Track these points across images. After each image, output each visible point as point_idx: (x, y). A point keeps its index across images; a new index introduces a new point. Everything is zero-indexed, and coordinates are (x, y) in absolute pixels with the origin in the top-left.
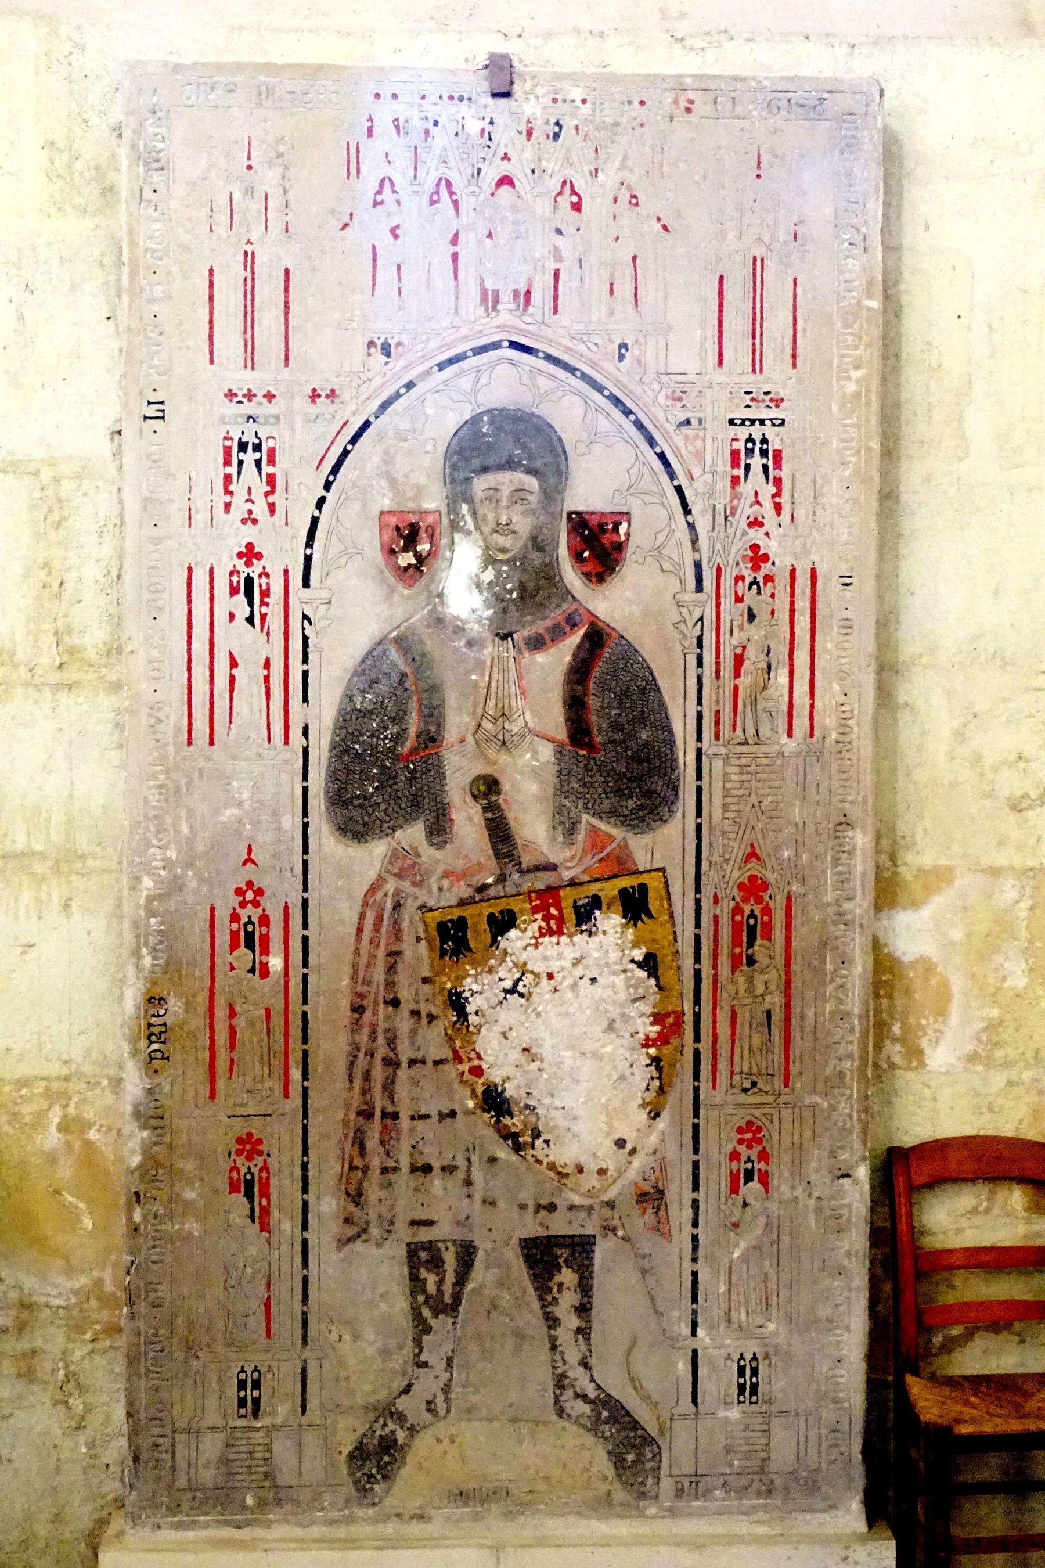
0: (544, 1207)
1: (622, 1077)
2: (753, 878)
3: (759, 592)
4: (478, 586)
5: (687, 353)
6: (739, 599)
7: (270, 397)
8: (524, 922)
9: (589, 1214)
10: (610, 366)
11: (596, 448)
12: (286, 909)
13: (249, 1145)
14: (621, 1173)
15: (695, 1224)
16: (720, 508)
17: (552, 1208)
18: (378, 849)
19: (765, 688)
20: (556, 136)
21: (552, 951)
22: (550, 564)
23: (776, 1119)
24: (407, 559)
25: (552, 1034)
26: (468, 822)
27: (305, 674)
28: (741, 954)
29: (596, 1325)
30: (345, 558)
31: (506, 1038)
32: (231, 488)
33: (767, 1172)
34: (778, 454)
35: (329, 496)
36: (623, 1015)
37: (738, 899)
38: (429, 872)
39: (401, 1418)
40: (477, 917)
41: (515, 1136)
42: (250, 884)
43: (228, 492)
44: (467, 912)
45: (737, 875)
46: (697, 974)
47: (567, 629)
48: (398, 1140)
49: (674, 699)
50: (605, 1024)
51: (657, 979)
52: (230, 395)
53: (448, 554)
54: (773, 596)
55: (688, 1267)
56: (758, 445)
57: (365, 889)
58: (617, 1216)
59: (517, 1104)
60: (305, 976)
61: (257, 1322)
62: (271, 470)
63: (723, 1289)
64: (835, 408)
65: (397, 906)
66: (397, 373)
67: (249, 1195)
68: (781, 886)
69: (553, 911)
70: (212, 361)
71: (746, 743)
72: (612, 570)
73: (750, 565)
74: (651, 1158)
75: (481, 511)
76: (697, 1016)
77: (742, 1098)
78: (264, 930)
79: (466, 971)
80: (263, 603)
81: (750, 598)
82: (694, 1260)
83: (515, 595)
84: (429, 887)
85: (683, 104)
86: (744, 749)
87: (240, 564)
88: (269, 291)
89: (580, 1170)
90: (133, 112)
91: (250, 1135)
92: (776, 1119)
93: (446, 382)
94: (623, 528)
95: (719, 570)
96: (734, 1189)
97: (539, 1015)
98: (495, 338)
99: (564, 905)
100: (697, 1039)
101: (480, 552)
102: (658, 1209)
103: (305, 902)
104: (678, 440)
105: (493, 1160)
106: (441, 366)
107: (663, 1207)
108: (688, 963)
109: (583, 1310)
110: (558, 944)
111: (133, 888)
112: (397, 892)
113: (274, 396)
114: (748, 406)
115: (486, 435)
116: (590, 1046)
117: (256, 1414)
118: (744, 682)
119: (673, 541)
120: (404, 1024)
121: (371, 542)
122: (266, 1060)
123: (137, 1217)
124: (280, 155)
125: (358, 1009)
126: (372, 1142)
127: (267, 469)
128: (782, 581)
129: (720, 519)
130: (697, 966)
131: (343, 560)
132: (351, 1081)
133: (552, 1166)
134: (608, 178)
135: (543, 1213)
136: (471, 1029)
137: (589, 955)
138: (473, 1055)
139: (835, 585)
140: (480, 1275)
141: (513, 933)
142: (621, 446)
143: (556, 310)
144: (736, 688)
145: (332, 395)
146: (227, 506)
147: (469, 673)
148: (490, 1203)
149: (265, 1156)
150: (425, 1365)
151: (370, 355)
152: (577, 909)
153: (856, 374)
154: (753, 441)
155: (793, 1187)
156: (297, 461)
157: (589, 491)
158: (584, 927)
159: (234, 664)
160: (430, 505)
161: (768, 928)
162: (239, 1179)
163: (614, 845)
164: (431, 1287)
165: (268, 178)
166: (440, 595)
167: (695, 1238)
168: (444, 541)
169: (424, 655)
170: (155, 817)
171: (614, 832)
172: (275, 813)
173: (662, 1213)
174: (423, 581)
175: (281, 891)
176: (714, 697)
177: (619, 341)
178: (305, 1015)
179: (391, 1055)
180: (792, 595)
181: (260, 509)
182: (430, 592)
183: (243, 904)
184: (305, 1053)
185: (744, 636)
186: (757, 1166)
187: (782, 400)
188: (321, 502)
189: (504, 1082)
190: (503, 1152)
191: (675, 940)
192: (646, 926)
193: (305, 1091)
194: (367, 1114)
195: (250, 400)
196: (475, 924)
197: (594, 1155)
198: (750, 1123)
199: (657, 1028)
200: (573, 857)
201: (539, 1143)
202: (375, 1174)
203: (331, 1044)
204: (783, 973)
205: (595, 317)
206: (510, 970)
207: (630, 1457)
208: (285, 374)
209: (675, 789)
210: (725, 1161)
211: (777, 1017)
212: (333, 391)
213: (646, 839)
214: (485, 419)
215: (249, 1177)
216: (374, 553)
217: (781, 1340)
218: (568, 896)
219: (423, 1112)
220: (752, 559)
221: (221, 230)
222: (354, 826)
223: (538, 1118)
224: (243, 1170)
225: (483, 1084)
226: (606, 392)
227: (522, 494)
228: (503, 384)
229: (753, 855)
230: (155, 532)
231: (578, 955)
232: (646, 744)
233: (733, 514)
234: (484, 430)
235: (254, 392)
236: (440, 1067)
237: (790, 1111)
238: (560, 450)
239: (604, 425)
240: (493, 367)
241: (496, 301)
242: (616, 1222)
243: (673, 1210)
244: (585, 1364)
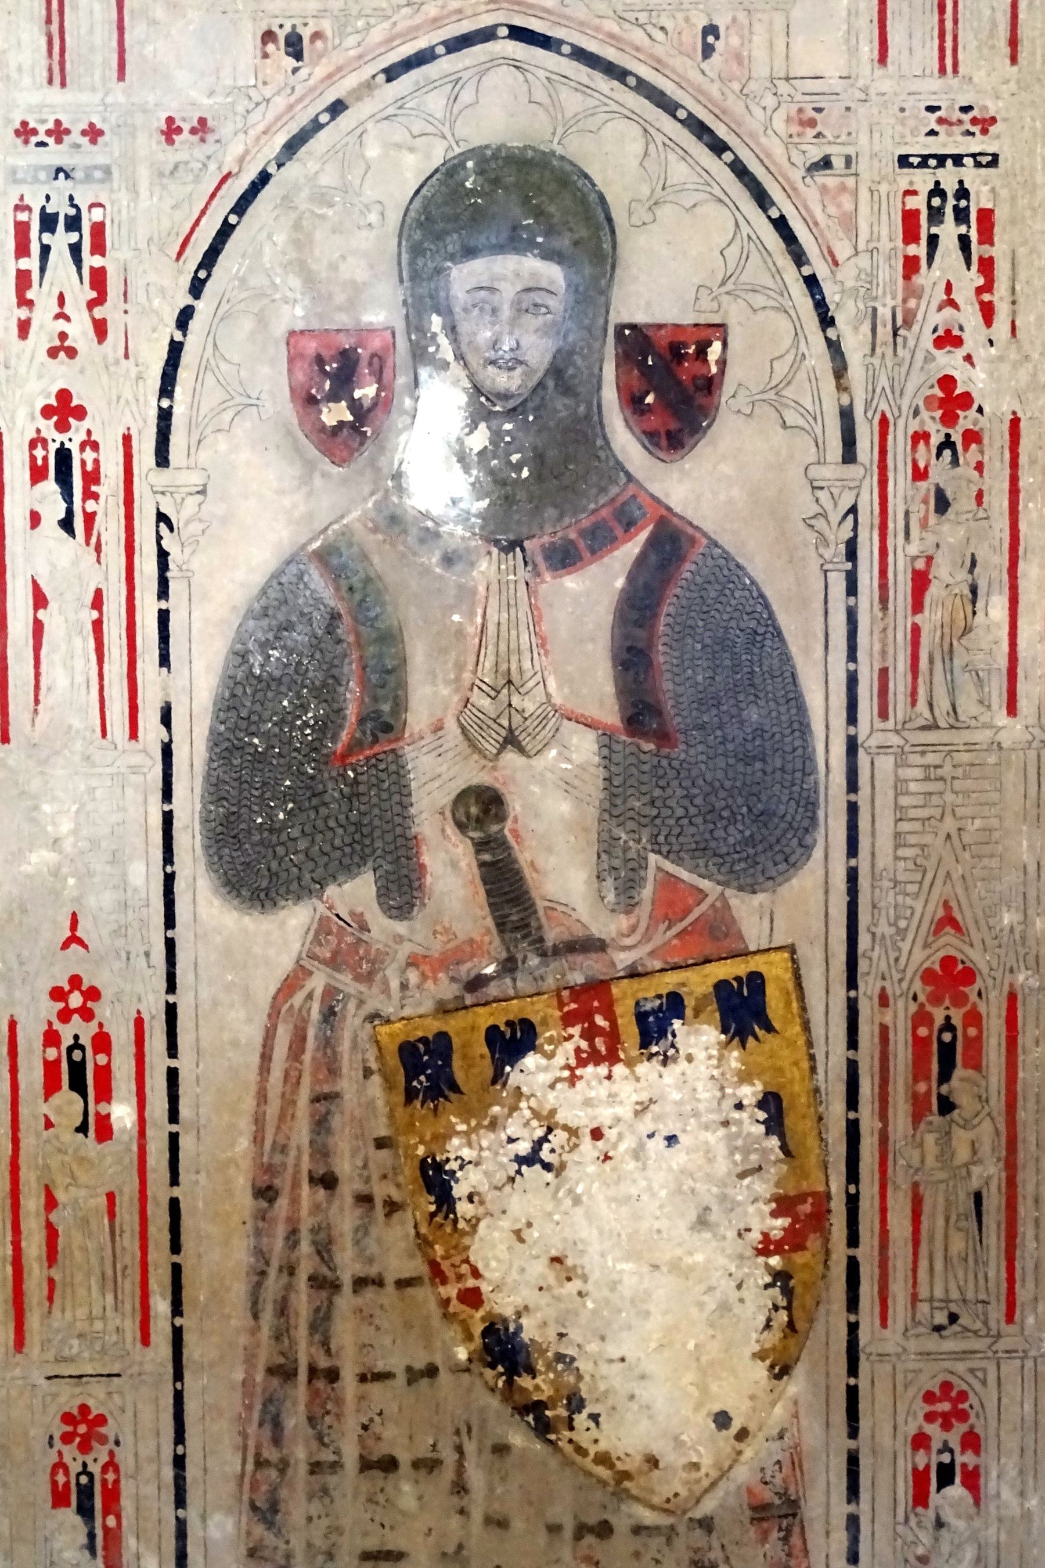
0: (591, 1530)
1: (724, 1307)
2: (948, 962)
3: (955, 462)
4: (462, 458)
6: (919, 474)
7: (93, 133)
8: (550, 1041)
9: (669, 1541)
10: (689, 67)
11: (665, 212)
12: (139, 1023)
13: (83, 1426)
16: (884, 313)
17: (604, 1530)
18: (296, 920)
19: (967, 630)
21: (602, 1091)
22: (588, 417)
23: (992, 1377)
24: (335, 413)
25: (601, 1232)
26: (449, 867)
27: (164, 617)
28: (928, 1093)
30: (230, 413)
31: (522, 1240)
32: (30, 295)
33: (977, 1468)
34: (986, 217)
35: (200, 305)
37: (922, 998)
40: (469, 1031)
41: (538, 1407)
42: (75, 981)
43: (24, 302)
44: (453, 1025)
45: (921, 957)
46: (853, 1130)
47: (619, 531)
48: (338, 1416)
49: (807, 650)
50: (692, 1215)
51: (782, 1137)
52: (25, 132)
53: (408, 402)
54: (979, 467)
56: (951, 202)
57: (272, 990)
58: (716, 1544)
59: (543, 1352)
60: (174, 1138)
62: (97, 261)
65: (329, 1015)
66: (312, 90)
67: (85, 1511)
68: (998, 975)
69: (600, 1021)
71: (934, 726)
73: (938, 414)
74: (776, 1445)
75: (464, 328)
76: (853, 1202)
77: (932, 1343)
79: (452, 1126)
80: (89, 495)
81: (940, 472)
83: (525, 473)
84: (386, 982)
86: (931, 737)
87: (48, 428)
89: (653, 1462)
91: (84, 1409)
92: (992, 1377)
93: (400, 102)
94: (715, 350)
95: (884, 422)
96: (921, 1498)
97: (577, 1201)
98: (486, 21)
99: (619, 1010)
100: (853, 1240)
101: (463, 399)
102: (789, 1531)
103: (171, 1011)
104: (811, 194)
105: (501, 1449)
106: (391, 73)
107: (796, 1530)
108: (836, 1109)
110: (609, 1077)
112: (330, 992)
113: (101, 133)
114: (932, 133)
115: (472, 192)
116: (665, 1254)
118: (930, 619)
119: (802, 375)
120: (345, 1219)
121: (272, 383)
122: (111, 1283)
125: (266, 1193)
126: (294, 1420)
127: (90, 260)
128: (997, 438)
129: (884, 332)
130: (852, 1115)
131: (227, 416)
132: (256, 1316)
133: (604, 1459)
135: (589, 1539)
136: (462, 1225)
137: (663, 1097)
138: (465, 1269)
141: (531, 1060)
142: (711, 209)
144: (916, 630)
145: (202, 128)
146: (24, 328)
148: (498, 1523)
149: (111, 1445)
151: (266, 56)
152: (641, 1017)
154: (942, 194)
155: (1022, 1494)
156: (142, 245)
157: (654, 288)
158: (654, 1049)
159: (40, 600)
161: (975, 1045)
162: (67, 1484)
163: (704, 907)
166: (397, 476)
168: (402, 380)
169: (368, 581)
171: (705, 884)
172: (115, 859)
173: (795, 1540)
175: (130, 992)
176: (877, 647)
177: (702, 22)
178: (174, 1205)
179: (325, 1271)
180: (1014, 464)
181: (80, 330)
182: (377, 470)
183: (65, 1016)
184: (177, 1270)
185: (931, 539)
186: (959, 1459)
187: (993, 120)
189: (519, 1315)
190: (519, 1437)
191: (813, 1069)
192: (763, 1046)
193: (177, 1334)
194: (283, 1372)
195: (59, 141)
196: (465, 1045)
197: (676, 1439)
198: (946, 1386)
200: (633, 929)
201: (581, 1420)
203: (221, 1251)
204: (1002, 1128)
206: (527, 1124)
208: (118, 94)
210: (904, 1448)
211: (994, 1202)
212: (202, 121)
213: (761, 898)
214: (470, 164)
215: (84, 1479)
218: (626, 997)
219: (380, 1366)
220: (942, 403)
222: (255, 875)
223: (580, 1377)
224: (75, 1468)
225: (483, 1319)
226: (682, 114)
227: (538, 297)
228: (499, 105)
229: (948, 921)
231: (644, 1096)
232: (760, 731)
233: (908, 323)
234: (468, 185)
235: (66, 125)
236: (410, 1291)
237: (1018, 1363)
238: (602, 217)
239: (679, 171)
240: (482, 74)
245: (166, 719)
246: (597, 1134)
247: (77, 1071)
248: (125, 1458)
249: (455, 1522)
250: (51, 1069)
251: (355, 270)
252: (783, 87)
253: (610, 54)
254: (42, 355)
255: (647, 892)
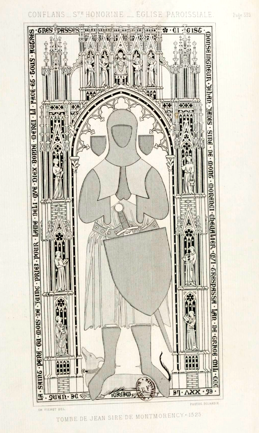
20: (133, 39)
67: (61, 316)
161: (193, 243)
198: (190, 294)
224: (60, 309)
250: (56, 248)
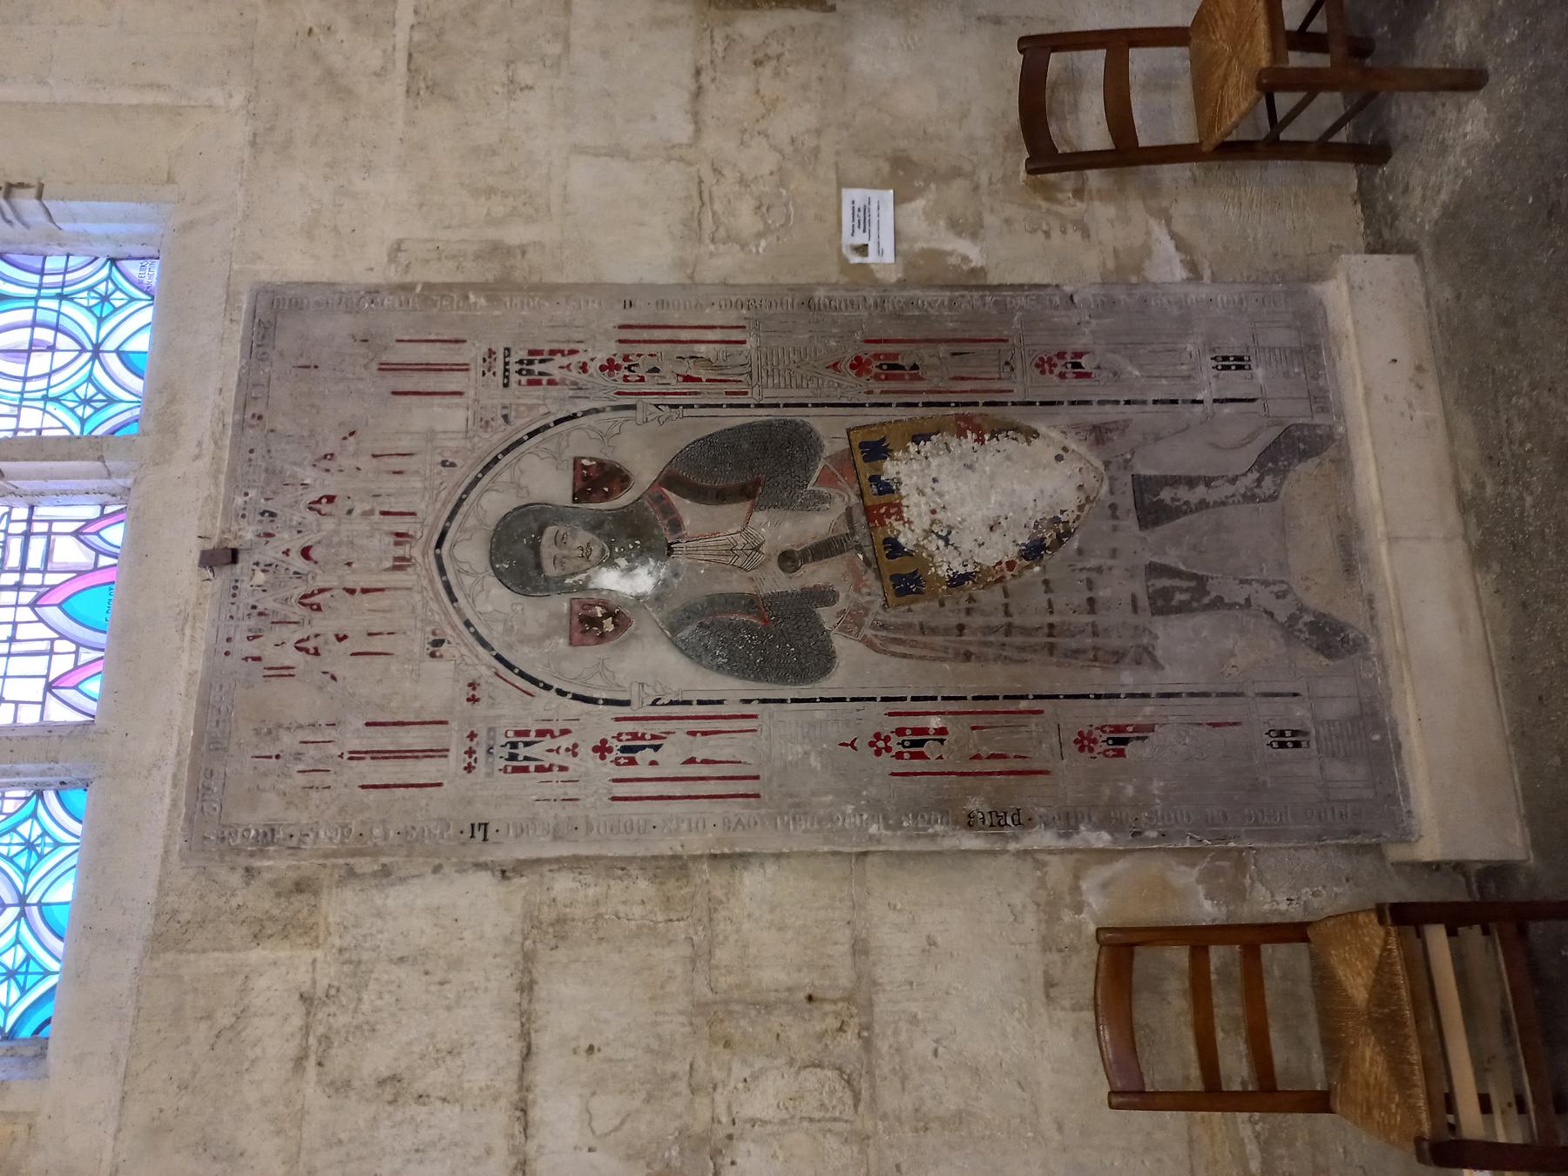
1: (1008, 458)
4: (630, 569)
5: (450, 418)
6: (642, 379)
7: (472, 736)
11: (523, 482)
12: (890, 714)
13: (1084, 742)
14: (1081, 458)
15: (1117, 402)
16: (571, 393)
18: (839, 643)
20: (272, 515)
21: (914, 510)
24: (608, 625)
26: (816, 575)
27: (700, 702)
29: (1203, 472)
34: (531, 353)
35: (556, 686)
36: (960, 458)
38: (856, 604)
39: (1293, 619)
42: (872, 744)
43: (550, 769)
44: (887, 574)
46: (927, 404)
50: (968, 472)
52: (469, 768)
55: (1150, 407)
60: (944, 698)
61: (1229, 734)
62: (533, 734)
63: (1164, 382)
64: (497, 313)
65: (884, 627)
67: (1125, 741)
70: (439, 785)
71: (750, 374)
72: (620, 470)
75: (572, 570)
77: (1018, 371)
78: (908, 732)
80: (643, 738)
81: (640, 371)
82: (1144, 402)
85: (255, 422)
87: (610, 757)
88: (382, 740)
90: (222, 855)
91: (1076, 742)
93: (466, 596)
94: (586, 462)
96: (1088, 375)
98: (432, 559)
100: (976, 404)
103: (884, 699)
105: (1080, 551)
106: (453, 600)
108: (919, 412)
109: (1191, 482)
111: (879, 841)
112: (873, 627)
117: (1306, 734)
118: (704, 374)
120: (977, 621)
121: (591, 654)
123: (1153, 834)
124: (270, 732)
125: (968, 656)
126: (1073, 644)
128: (627, 349)
129: (581, 393)
133: (1081, 508)
134: (309, 475)
139: (632, 312)
140: (1172, 558)
141: (902, 540)
142: (523, 464)
143: (413, 514)
145: (473, 685)
146: (563, 769)
147: (698, 574)
150: (1248, 600)
152: (880, 493)
153: (472, 298)
159: (692, 761)
160: (566, 606)
161: (887, 356)
164: (1185, 597)
165: (288, 741)
166: (638, 598)
167: (1128, 402)
168: (594, 596)
169: (685, 610)
170: (819, 823)
171: (820, 467)
174: (626, 611)
175: (876, 718)
178: (975, 698)
181: (565, 742)
183: (888, 749)
184: (1006, 697)
188: (561, 693)
190: (1074, 544)
193: (1036, 697)
194: (1051, 649)
198: (1037, 366)
199: (969, 433)
201: (1063, 518)
202: (1099, 641)
205: (419, 485)
207: (1302, 446)
208: (454, 725)
209: (785, 423)
211: (956, 348)
213: (825, 442)
216: (602, 650)
217: (1199, 341)
219: (1045, 605)
221: (329, 779)
222: (823, 661)
228: (470, 553)
230: (582, 828)
239: (505, 477)
241: (403, 559)
242: (1120, 460)
243: (1109, 418)
244: (1234, 480)
245: (748, 701)
246: (933, 512)
247: (914, 744)
248: (1097, 722)
249: (1116, 572)
250: (914, 756)
251: (543, 615)
252: (471, 434)
253: (450, 507)
254: (576, 760)
255: (824, 490)
